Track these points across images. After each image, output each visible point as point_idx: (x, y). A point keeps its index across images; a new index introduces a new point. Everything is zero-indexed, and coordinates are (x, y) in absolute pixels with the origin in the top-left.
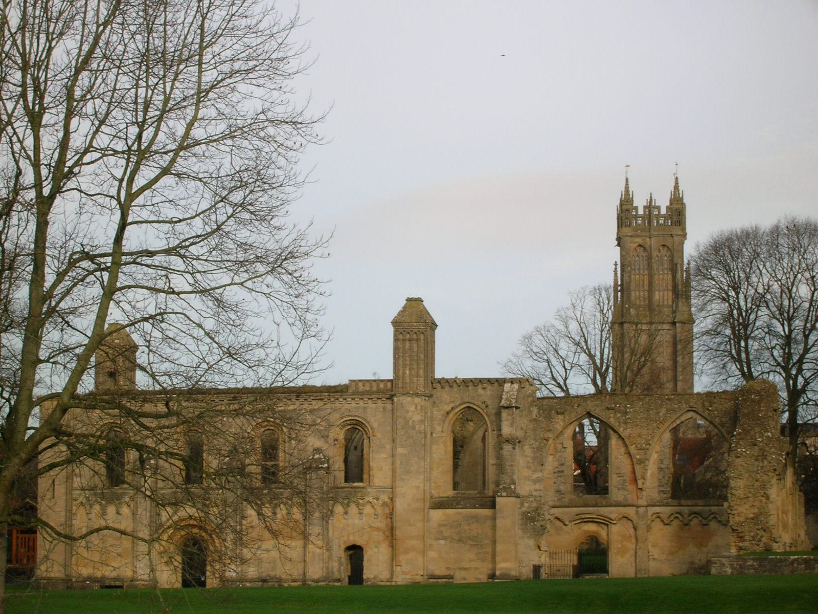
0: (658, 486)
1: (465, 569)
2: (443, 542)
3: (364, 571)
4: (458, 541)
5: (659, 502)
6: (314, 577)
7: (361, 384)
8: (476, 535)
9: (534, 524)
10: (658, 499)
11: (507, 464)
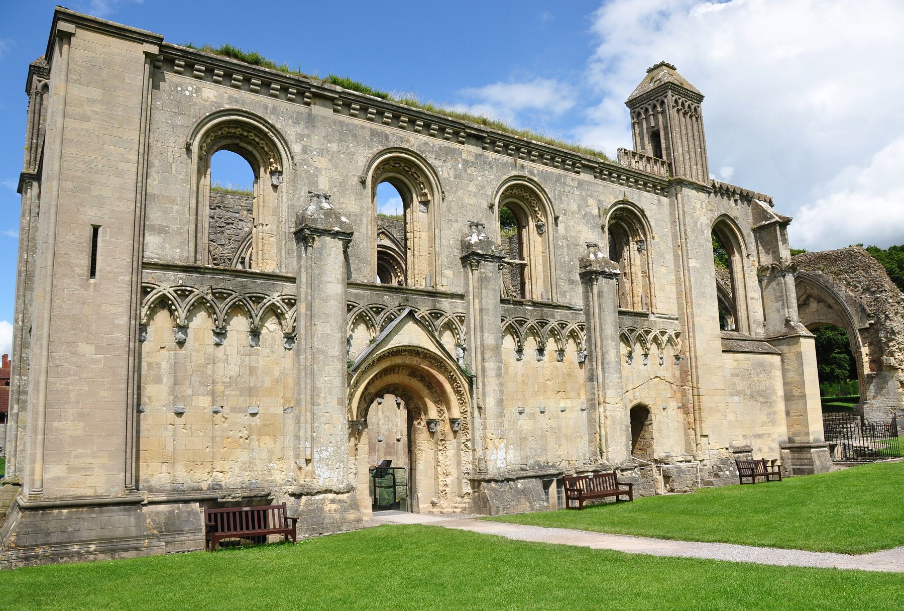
2: (736, 399)
6: (616, 461)
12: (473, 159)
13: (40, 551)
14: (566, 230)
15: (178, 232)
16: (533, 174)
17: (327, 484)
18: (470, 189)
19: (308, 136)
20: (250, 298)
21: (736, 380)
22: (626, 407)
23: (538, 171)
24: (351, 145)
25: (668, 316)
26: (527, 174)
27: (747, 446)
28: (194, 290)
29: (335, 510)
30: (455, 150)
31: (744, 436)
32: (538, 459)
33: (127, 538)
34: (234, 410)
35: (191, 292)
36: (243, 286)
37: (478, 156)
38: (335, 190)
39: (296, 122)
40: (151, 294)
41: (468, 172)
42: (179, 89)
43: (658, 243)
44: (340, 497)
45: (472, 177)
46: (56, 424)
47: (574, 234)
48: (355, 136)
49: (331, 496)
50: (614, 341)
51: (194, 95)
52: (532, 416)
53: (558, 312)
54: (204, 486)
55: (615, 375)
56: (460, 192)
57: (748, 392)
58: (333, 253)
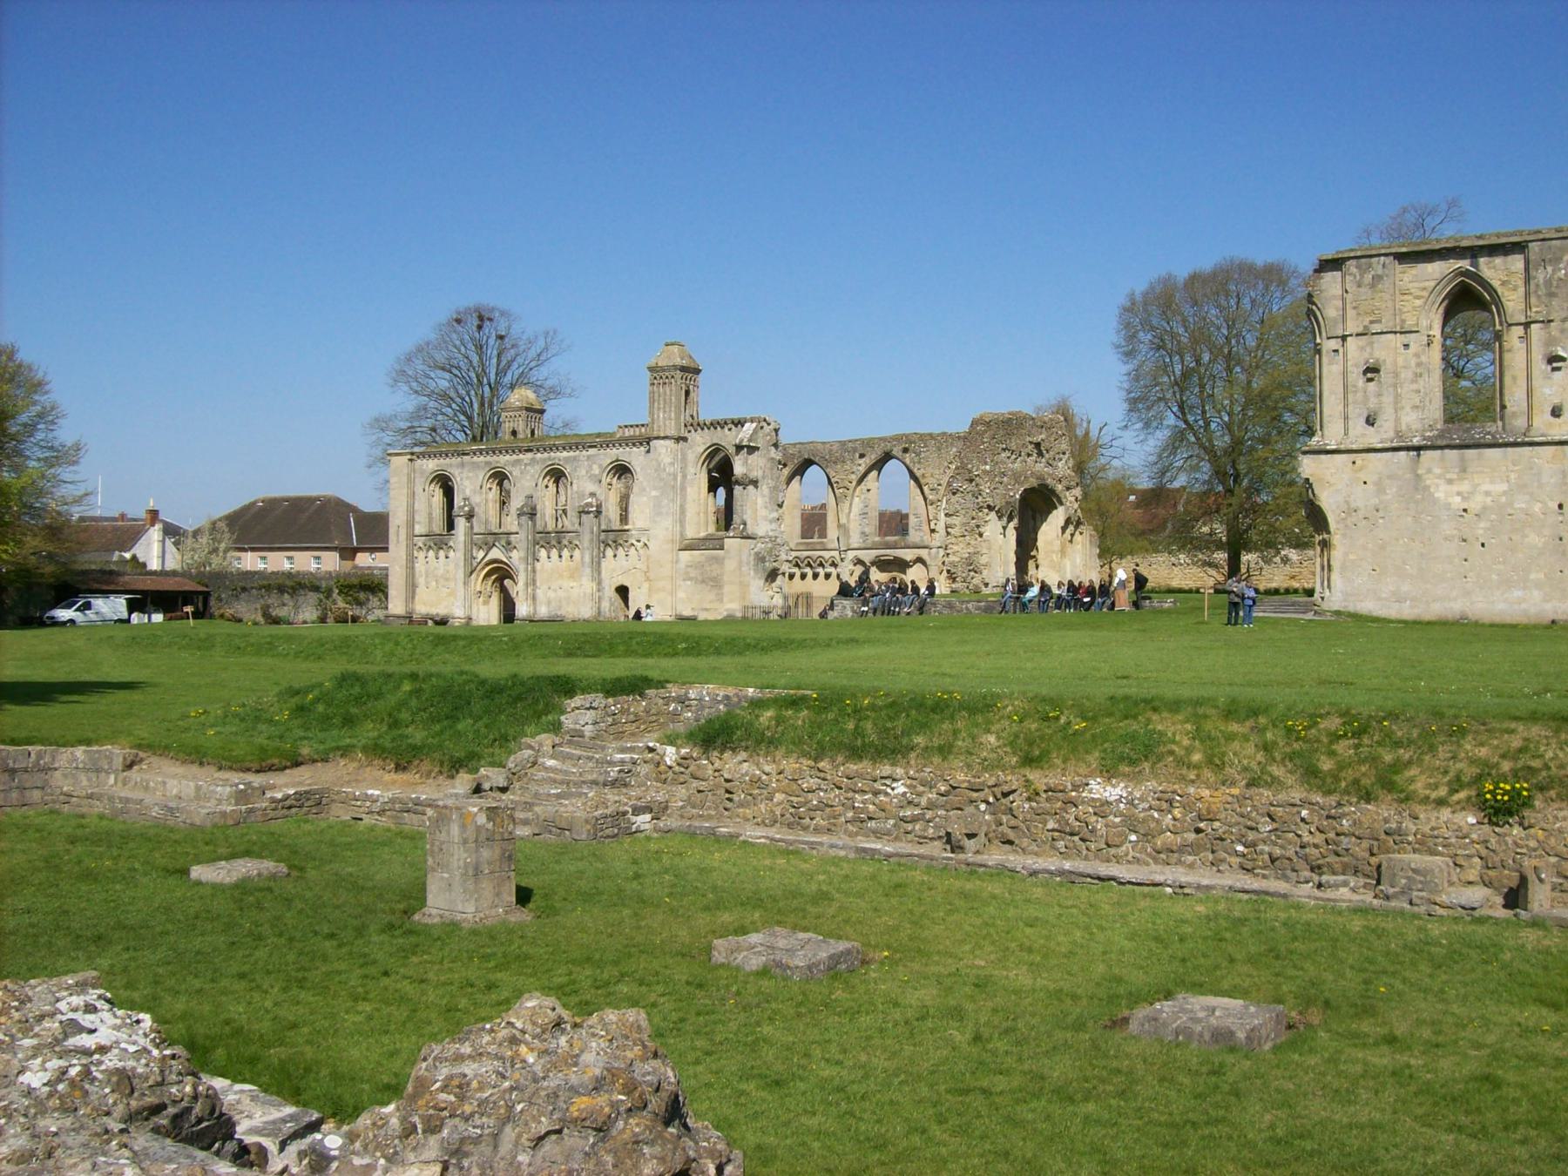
52: (555, 591)
57: (700, 578)
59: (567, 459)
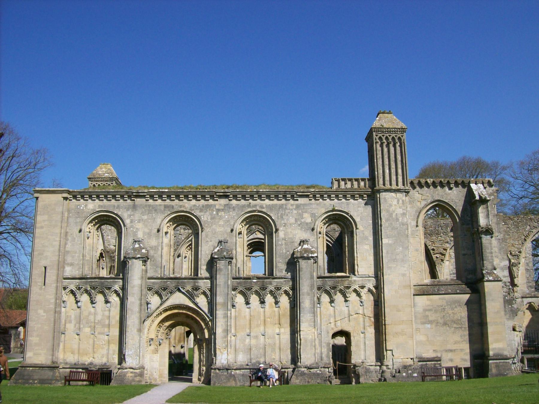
0: (527, 283)
1: (451, 351)
2: (429, 326)
3: (352, 357)
4: (443, 325)
5: (528, 294)
6: (306, 363)
7: (342, 183)
8: (459, 318)
9: (512, 307)
10: (528, 292)
11: (488, 251)
12: (223, 208)
13: (20, 381)
14: (285, 235)
15: (78, 264)
16: (263, 208)
17: (131, 365)
18: (220, 223)
19: (133, 215)
20: (106, 288)
21: (427, 313)
22: (328, 333)
23: (266, 205)
24: (154, 215)
25: (368, 276)
26: (258, 208)
27: (437, 357)
28: (83, 287)
29: (131, 376)
30: (211, 205)
31: (434, 351)
32: (259, 360)
33: (48, 380)
34: (99, 333)
35: (82, 287)
36: (102, 283)
37: (225, 205)
38: (146, 237)
39: (128, 210)
40: (67, 289)
41: (219, 214)
42: (79, 207)
43: (363, 231)
44: (136, 371)
45: (222, 217)
46: (30, 338)
47: (291, 236)
48: (156, 210)
49: (132, 370)
50: (309, 295)
51: (84, 208)
52: (256, 337)
53: (275, 281)
54: (87, 363)
55: (309, 315)
56: (214, 226)
57: (441, 321)
58: (137, 267)
59: (270, 207)
